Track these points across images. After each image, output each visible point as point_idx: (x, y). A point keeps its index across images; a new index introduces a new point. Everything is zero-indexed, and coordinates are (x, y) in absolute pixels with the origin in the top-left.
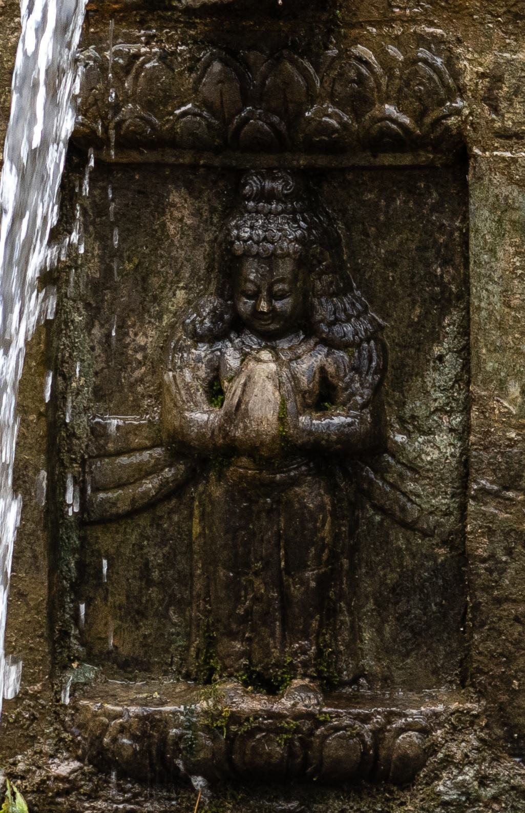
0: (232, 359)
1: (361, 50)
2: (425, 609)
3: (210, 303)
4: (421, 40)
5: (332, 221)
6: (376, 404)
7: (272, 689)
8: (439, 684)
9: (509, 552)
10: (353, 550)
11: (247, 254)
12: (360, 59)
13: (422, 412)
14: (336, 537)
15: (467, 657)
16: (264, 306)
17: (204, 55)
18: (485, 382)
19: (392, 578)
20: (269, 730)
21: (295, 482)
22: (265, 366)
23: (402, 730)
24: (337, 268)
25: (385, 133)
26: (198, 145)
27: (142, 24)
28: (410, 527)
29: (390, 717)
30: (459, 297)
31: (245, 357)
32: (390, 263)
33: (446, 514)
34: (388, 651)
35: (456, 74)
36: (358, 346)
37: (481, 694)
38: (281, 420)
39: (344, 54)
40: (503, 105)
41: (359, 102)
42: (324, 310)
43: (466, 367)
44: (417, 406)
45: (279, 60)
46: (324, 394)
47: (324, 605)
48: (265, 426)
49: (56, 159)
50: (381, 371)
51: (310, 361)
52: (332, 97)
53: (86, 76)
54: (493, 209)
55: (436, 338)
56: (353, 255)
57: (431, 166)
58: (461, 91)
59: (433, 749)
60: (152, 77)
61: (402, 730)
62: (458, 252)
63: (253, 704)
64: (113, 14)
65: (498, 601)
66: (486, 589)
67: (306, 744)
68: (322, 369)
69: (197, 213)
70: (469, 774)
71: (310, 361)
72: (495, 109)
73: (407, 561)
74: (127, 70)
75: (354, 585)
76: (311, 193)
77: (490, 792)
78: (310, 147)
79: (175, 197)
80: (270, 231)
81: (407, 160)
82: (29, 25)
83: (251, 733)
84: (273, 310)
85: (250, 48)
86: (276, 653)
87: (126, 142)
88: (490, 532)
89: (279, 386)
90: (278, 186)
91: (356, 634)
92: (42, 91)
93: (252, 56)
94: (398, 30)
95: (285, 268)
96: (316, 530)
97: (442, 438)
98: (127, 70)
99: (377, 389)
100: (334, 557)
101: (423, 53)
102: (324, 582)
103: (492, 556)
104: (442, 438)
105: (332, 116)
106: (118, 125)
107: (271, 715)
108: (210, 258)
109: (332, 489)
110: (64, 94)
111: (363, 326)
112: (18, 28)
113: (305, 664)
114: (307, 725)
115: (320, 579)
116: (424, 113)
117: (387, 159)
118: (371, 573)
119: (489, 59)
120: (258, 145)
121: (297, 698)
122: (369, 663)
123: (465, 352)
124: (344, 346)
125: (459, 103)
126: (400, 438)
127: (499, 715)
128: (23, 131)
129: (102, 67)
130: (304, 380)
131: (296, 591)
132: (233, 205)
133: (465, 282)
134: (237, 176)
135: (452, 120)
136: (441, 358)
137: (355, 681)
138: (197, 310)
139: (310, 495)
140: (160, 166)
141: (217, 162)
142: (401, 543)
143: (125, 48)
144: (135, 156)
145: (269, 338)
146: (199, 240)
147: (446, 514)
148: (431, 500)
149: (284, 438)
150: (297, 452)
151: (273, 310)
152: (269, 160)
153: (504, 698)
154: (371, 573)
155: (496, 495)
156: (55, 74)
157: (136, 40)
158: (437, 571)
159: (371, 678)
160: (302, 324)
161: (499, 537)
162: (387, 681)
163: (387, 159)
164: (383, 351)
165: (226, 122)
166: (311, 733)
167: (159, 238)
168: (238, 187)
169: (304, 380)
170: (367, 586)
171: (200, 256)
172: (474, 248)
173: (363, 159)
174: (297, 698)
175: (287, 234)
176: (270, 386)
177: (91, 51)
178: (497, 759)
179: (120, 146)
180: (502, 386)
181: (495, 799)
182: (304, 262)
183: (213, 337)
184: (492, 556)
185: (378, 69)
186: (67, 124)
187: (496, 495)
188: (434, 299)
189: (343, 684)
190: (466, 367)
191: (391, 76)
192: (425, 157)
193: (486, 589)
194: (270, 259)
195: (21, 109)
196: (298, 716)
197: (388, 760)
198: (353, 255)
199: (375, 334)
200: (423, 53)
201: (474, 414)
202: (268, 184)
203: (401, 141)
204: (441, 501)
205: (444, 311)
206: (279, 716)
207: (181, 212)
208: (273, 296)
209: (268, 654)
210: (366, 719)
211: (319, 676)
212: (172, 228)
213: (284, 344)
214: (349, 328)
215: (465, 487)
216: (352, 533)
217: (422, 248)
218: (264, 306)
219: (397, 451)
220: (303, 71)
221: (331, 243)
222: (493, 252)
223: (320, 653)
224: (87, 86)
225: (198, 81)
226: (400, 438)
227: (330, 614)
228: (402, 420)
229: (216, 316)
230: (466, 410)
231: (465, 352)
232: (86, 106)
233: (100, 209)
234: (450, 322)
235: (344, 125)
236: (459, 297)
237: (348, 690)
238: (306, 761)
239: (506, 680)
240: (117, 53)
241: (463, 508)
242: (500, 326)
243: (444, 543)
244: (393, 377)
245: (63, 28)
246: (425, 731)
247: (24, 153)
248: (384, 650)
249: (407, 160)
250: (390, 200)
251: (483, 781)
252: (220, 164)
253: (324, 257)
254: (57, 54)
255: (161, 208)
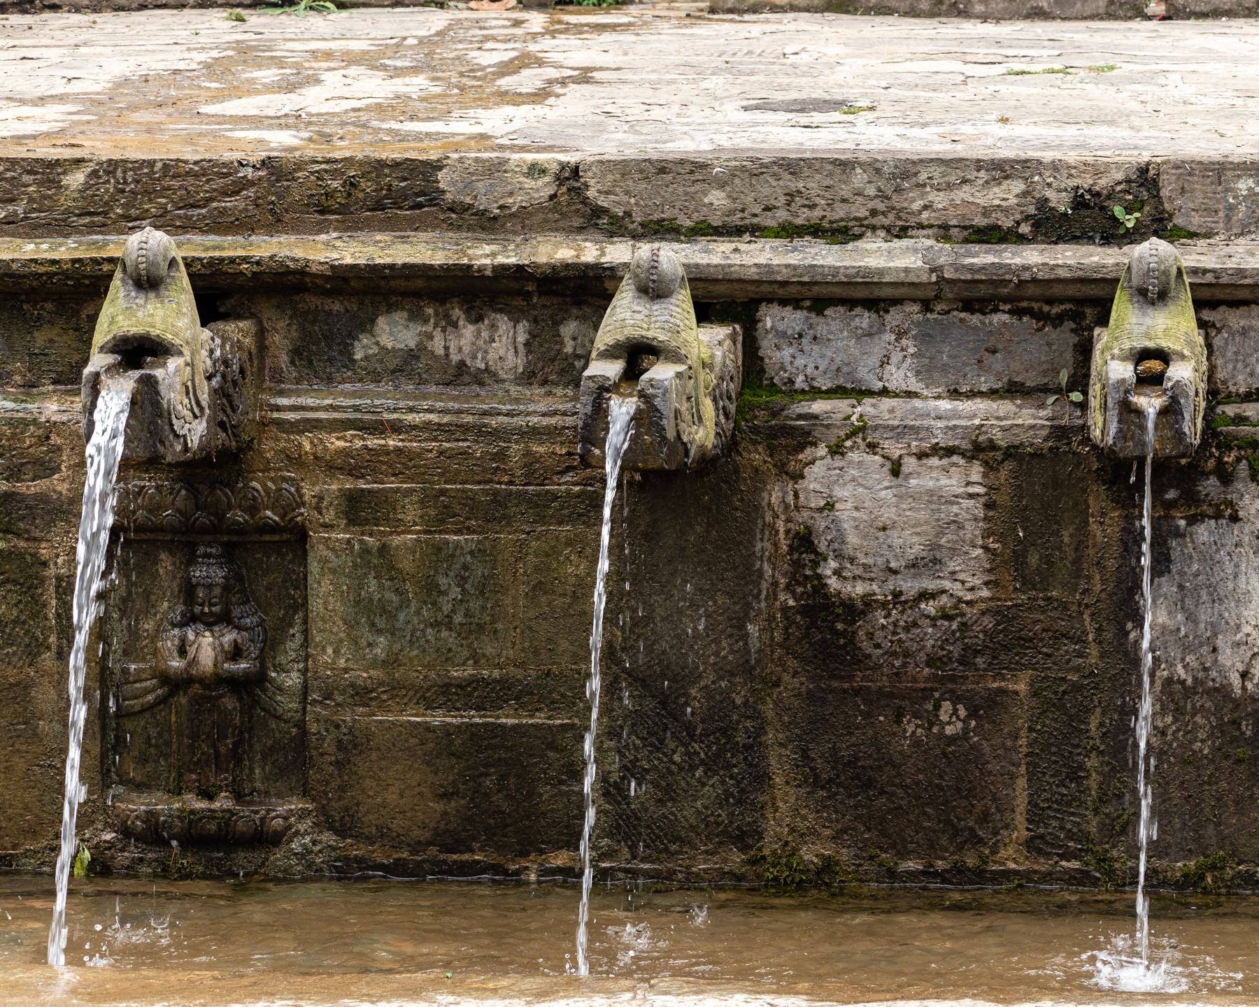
0: (191, 636)
1: (254, 484)
2: (286, 758)
3: (180, 608)
4: (284, 479)
5: (240, 568)
6: (262, 658)
7: (211, 797)
8: (292, 795)
9: (327, 730)
10: (251, 729)
11: (198, 584)
12: (254, 489)
13: (284, 662)
14: (242, 723)
15: (307, 781)
16: (206, 610)
17: (177, 486)
18: (315, 647)
19: (269, 743)
20: (209, 818)
21: (222, 696)
22: (207, 639)
23: (274, 818)
24: (243, 591)
25: (266, 524)
26: (175, 531)
27: (147, 471)
28: (278, 718)
29: (268, 811)
30: (302, 605)
31: (197, 634)
32: (269, 589)
33: (296, 712)
34: (268, 779)
35: (301, 496)
36: (253, 629)
37: (313, 800)
38: (215, 665)
39: (246, 486)
40: (324, 511)
41: (253, 509)
42: (236, 612)
43: (306, 639)
44: (282, 659)
45: (214, 489)
46: (236, 653)
47: (236, 756)
48: (207, 669)
49: (104, 537)
50: (264, 641)
51: (229, 637)
52: (240, 507)
53: (119, 497)
54: (319, 562)
55: (291, 625)
56: (250, 585)
57: (288, 541)
58: (303, 504)
59: (290, 827)
60: (152, 497)
61: (274, 818)
62: (302, 583)
63: (201, 805)
64: (132, 466)
65: (322, 755)
66: (316, 748)
67: (227, 825)
68: (235, 641)
69: (174, 564)
70: (307, 839)
71: (229, 637)
72: (320, 513)
73: (277, 735)
74: (139, 493)
75: (251, 746)
76: (230, 554)
77: (317, 848)
78: (229, 532)
79: (163, 556)
80: (209, 573)
81: (277, 538)
82: (91, 472)
83: (200, 819)
84: (211, 611)
85: (201, 483)
86: (213, 780)
87: (139, 529)
88: (318, 721)
89: (214, 649)
90: (214, 551)
91: (252, 770)
92: (97, 504)
93: (201, 487)
94: (273, 474)
95: (217, 591)
96: (232, 720)
97: (294, 675)
98: (139, 493)
99: (262, 650)
100: (241, 732)
101: (285, 485)
102: (236, 745)
103: (319, 732)
104: (294, 675)
105: (240, 516)
106: (135, 521)
107: (210, 810)
108: (180, 586)
109: (240, 699)
110: (108, 506)
111: (255, 620)
112: (86, 473)
113: (227, 786)
114: (227, 816)
115: (234, 744)
116: (285, 515)
117: (267, 538)
118: (259, 741)
119: (317, 488)
120: (203, 531)
121: (223, 802)
122: (258, 785)
123: (306, 632)
124: (246, 629)
125: (303, 510)
126: (273, 674)
127: (323, 810)
128: (479, 483)
129: (127, 492)
130: (226, 646)
131: (222, 749)
132: (191, 560)
133: (306, 598)
134: (193, 546)
135: (299, 518)
136: (293, 635)
137: (251, 794)
138: (174, 612)
139: (229, 703)
140: (156, 540)
141: (183, 539)
142: (274, 726)
143: (138, 483)
144: (143, 536)
145: (209, 626)
146: (174, 577)
147: (296, 712)
148: (289, 705)
149: (216, 674)
150: (223, 681)
151: (211, 611)
152: (209, 538)
153: (325, 802)
154: (259, 741)
155: (321, 702)
156: (104, 496)
157: (144, 479)
158: (291, 740)
159: (259, 792)
160: (224, 619)
161: (322, 723)
162: (267, 794)
163: (267, 538)
164: (265, 631)
165: (188, 520)
166: (230, 819)
167: (155, 576)
168: (194, 551)
169: (226, 646)
170: (257, 747)
171: (175, 585)
172: (310, 582)
173: (255, 538)
174: (223, 802)
175: (218, 574)
176: (209, 649)
177: (122, 484)
178: (321, 832)
179: (136, 531)
180: (324, 648)
181: (320, 851)
182: (226, 588)
183: (181, 625)
184: (319, 732)
185: (263, 493)
186: (110, 520)
187: (321, 702)
188: (290, 606)
189: (246, 795)
190: (306, 639)
191: (269, 497)
192: (286, 536)
193: (316, 748)
194: (210, 587)
195: (87, 513)
196: (224, 811)
197: (268, 833)
198: (250, 585)
199: (261, 623)
200: (285, 485)
201: (310, 662)
202: (209, 550)
203: (273, 528)
204: (293, 705)
205: (295, 612)
206: (214, 811)
207: (166, 564)
208: (211, 605)
209: (208, 781)
210: (256, 812)
211: (234, 791)
212: (161, 571)
213: (216, 628)
214: (248, 621)
215: (305, 698)
216: (249, 721)
217: (285, 581)
218: (206, 610)
219: (272, 681)
220: (226, 494)
221: (240, 579)
222: (319, 583)
223: (234, 780)
224: (120, 502)
225: (174, 499)
226: (273, 674)
227: (239, 761)
228: (274, 666)
229: (183, 615)
230: (306, 661)
231: (306, 632)
232: (118, 512)
233: (126, 562)
234: (298, 618)
235: (246, 521)
236: (303, 605)
237: (248, 798)
238: (227, 833)
239: (326, 794)
240: (135, 486)
241: (304, 709)
242: (323, 619)
243: (295, 726)
244: (270, 644)
245: (108, 473)
246: (286, 818)
247: (89, 535)
248: (266, 779)
249: (277, 538)
250: (269, 558)
251: (314, 842)
252: (185, 540)
253: (237, 586)
254: (105, 486)
255: (156, 562)
